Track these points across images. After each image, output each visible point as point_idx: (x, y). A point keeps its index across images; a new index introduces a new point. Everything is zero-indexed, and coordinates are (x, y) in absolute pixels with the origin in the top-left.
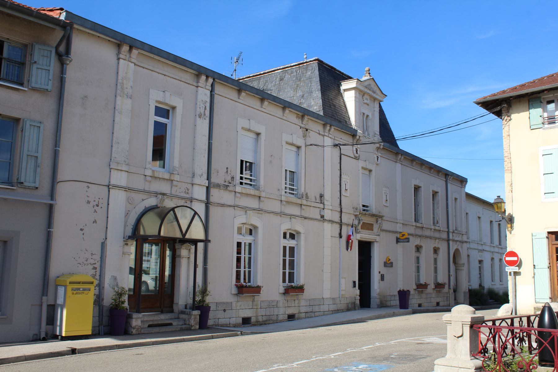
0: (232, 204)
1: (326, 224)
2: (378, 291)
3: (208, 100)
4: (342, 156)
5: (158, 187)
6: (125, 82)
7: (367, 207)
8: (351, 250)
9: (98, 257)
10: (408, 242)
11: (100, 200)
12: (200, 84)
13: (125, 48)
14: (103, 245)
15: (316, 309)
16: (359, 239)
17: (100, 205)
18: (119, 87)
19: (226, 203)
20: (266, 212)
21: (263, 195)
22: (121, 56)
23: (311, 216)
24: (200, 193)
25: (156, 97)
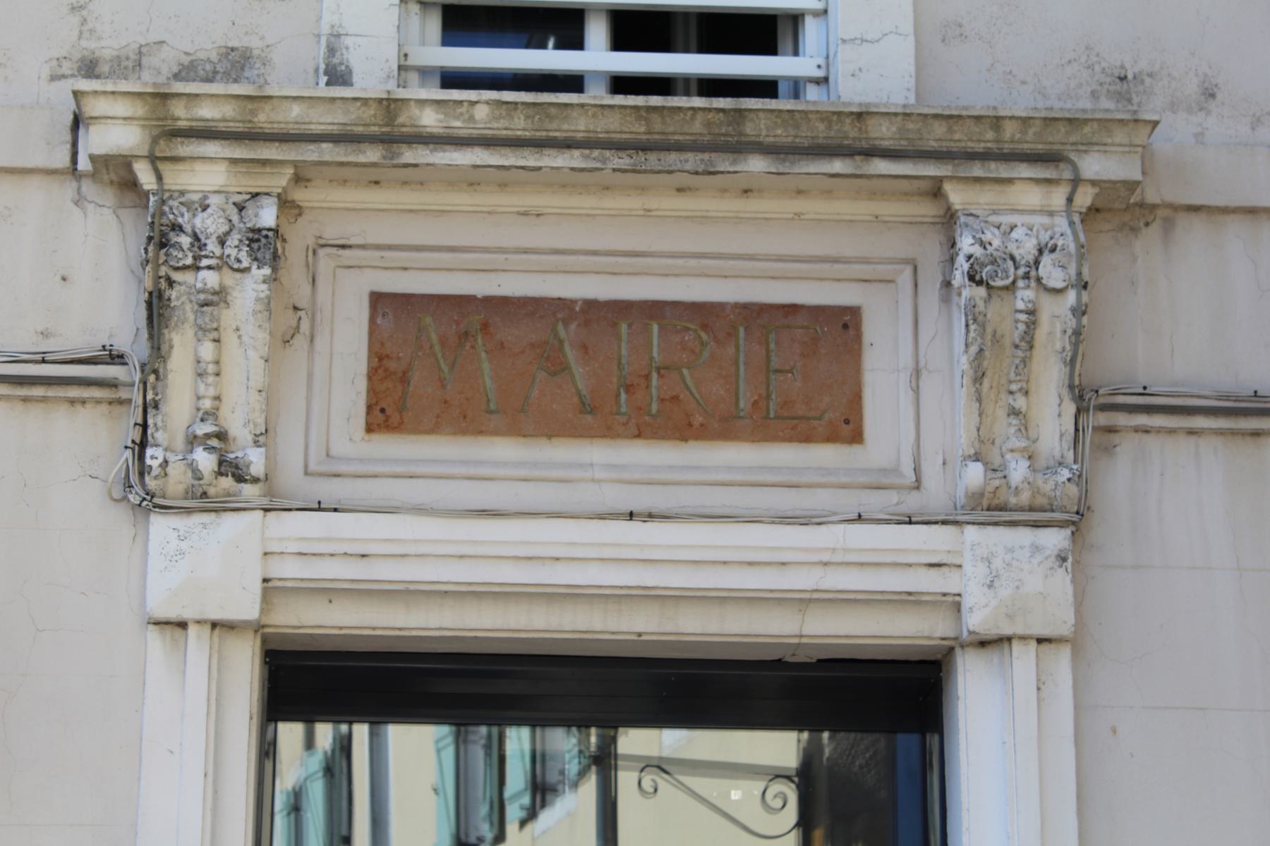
16: (247, 607)
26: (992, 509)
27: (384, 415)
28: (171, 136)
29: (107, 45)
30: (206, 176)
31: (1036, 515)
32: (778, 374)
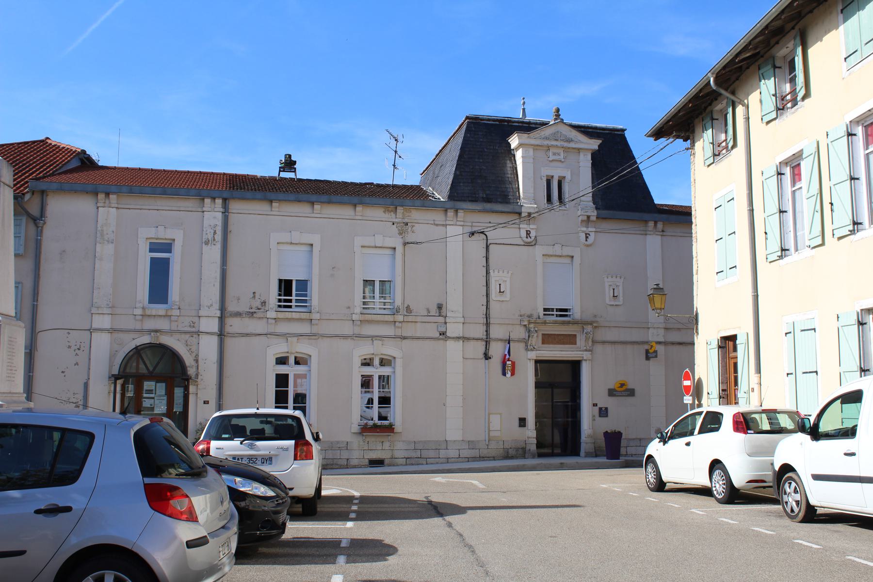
0: (265, 332)
1: (450, 344)
2: (590, 432)
3: (219, 223)
4: (491, 247)
5: (150, 324)
6: (105, 228)
7: (566, 310)
8: (513, 374)
9: (80, 397)
10: (656, 357)
11: (82, 345)
12: (204, 209)
13: (101, 196)
14: (86, 386)
15: (425, 454)
17: (82, 349)
18: (98, 235)
19: (254, 332)
20: (323, 336)
21: (315, 316)
22: (99, 205)
23: (418, 335)
24: (213, 325)
25: (147, 234)
26: (586, 350)
27: (543, 343)
28: (530, 323)
29: (522, 313)
30: (532, 326)
31: (589, 351)
32: (570, 340)
